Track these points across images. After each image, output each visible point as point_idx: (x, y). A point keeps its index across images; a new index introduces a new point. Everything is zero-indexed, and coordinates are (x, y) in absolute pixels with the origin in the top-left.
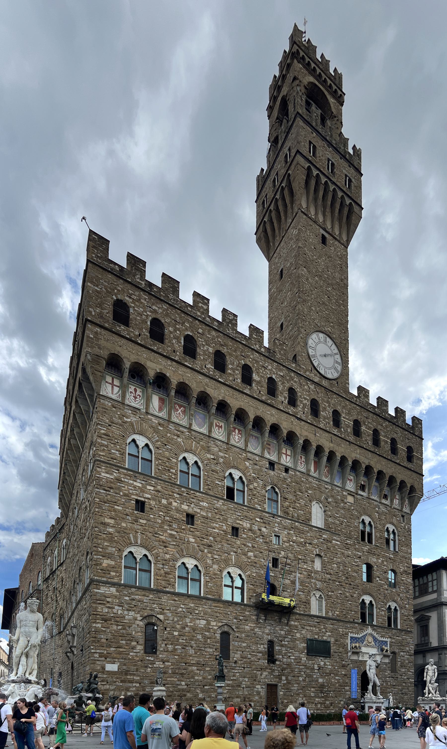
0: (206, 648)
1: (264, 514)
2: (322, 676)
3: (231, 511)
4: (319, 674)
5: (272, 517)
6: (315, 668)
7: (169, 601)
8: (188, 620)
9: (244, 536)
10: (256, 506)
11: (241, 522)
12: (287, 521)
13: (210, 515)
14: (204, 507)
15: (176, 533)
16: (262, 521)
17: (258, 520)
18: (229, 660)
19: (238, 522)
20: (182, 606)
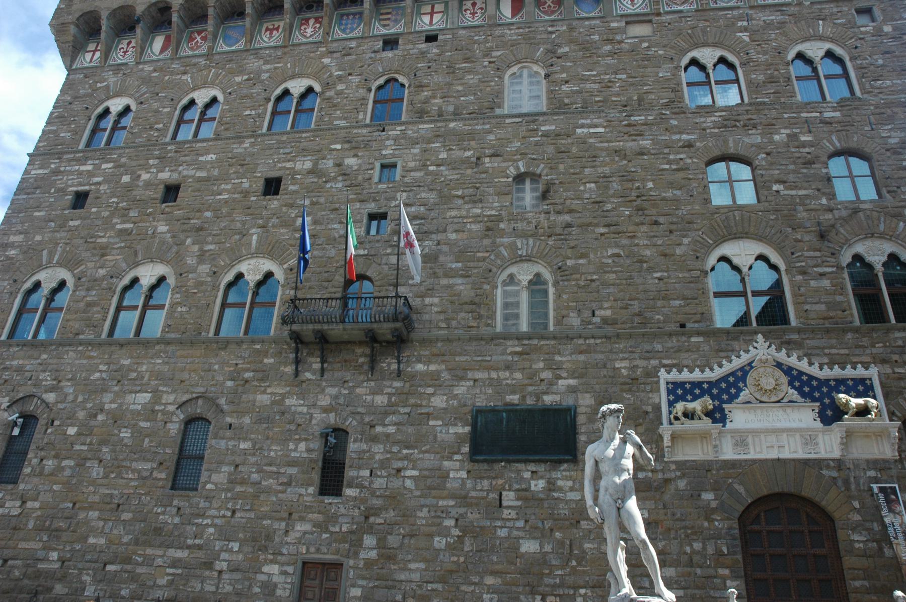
0: (135, 460)
1: (355, 131)
2: (535, 532)
3: (268, 152)
4: (520, 524)
5: (378, 130)
6: (505, 503)
7: (77, 362)
8: (107, 397)
9: (292, 188)
10: (338, 122)
11: (289, 165)
12: (421, 126)
13: (216, 172)
14: (207, 162)
15: (131, 225)
16: (346, 146)
17: (338, 147)
18: (196, 489)
19: (280, 165)
20: (102, 367)
